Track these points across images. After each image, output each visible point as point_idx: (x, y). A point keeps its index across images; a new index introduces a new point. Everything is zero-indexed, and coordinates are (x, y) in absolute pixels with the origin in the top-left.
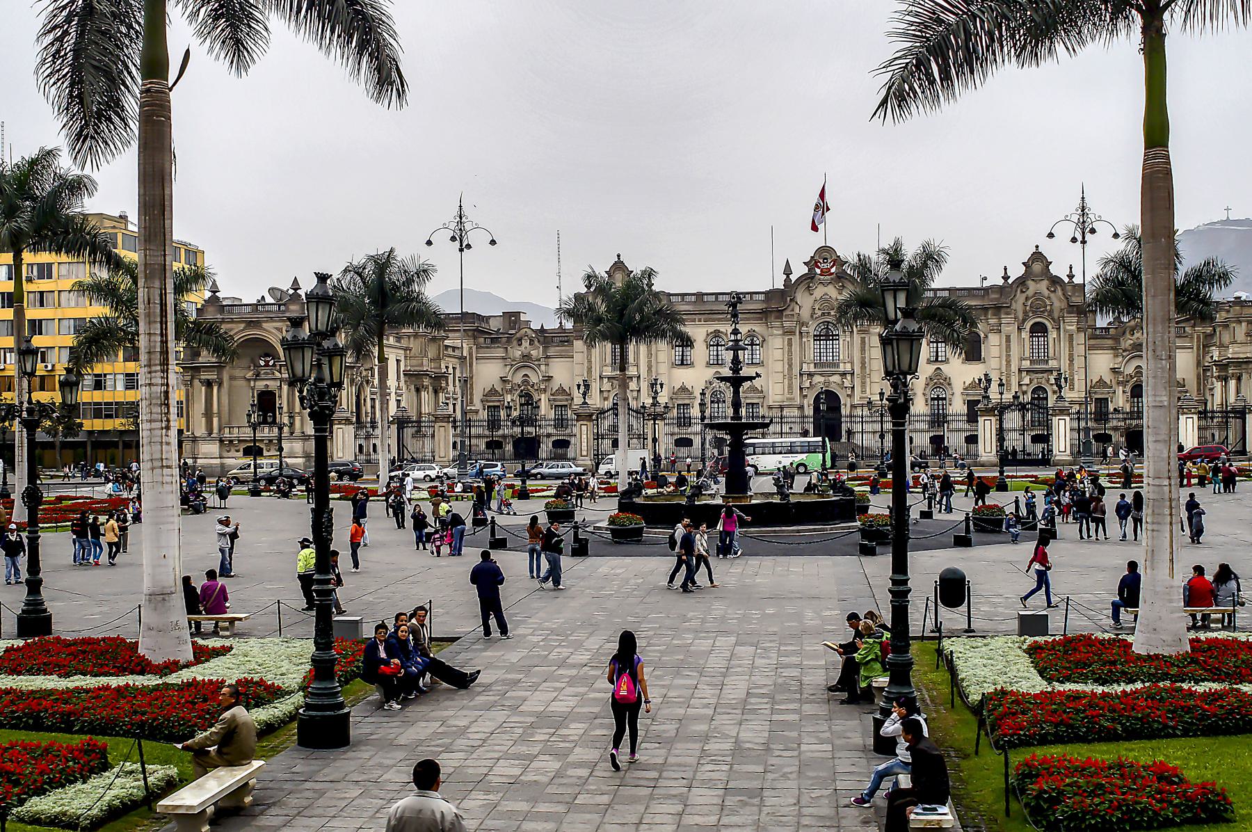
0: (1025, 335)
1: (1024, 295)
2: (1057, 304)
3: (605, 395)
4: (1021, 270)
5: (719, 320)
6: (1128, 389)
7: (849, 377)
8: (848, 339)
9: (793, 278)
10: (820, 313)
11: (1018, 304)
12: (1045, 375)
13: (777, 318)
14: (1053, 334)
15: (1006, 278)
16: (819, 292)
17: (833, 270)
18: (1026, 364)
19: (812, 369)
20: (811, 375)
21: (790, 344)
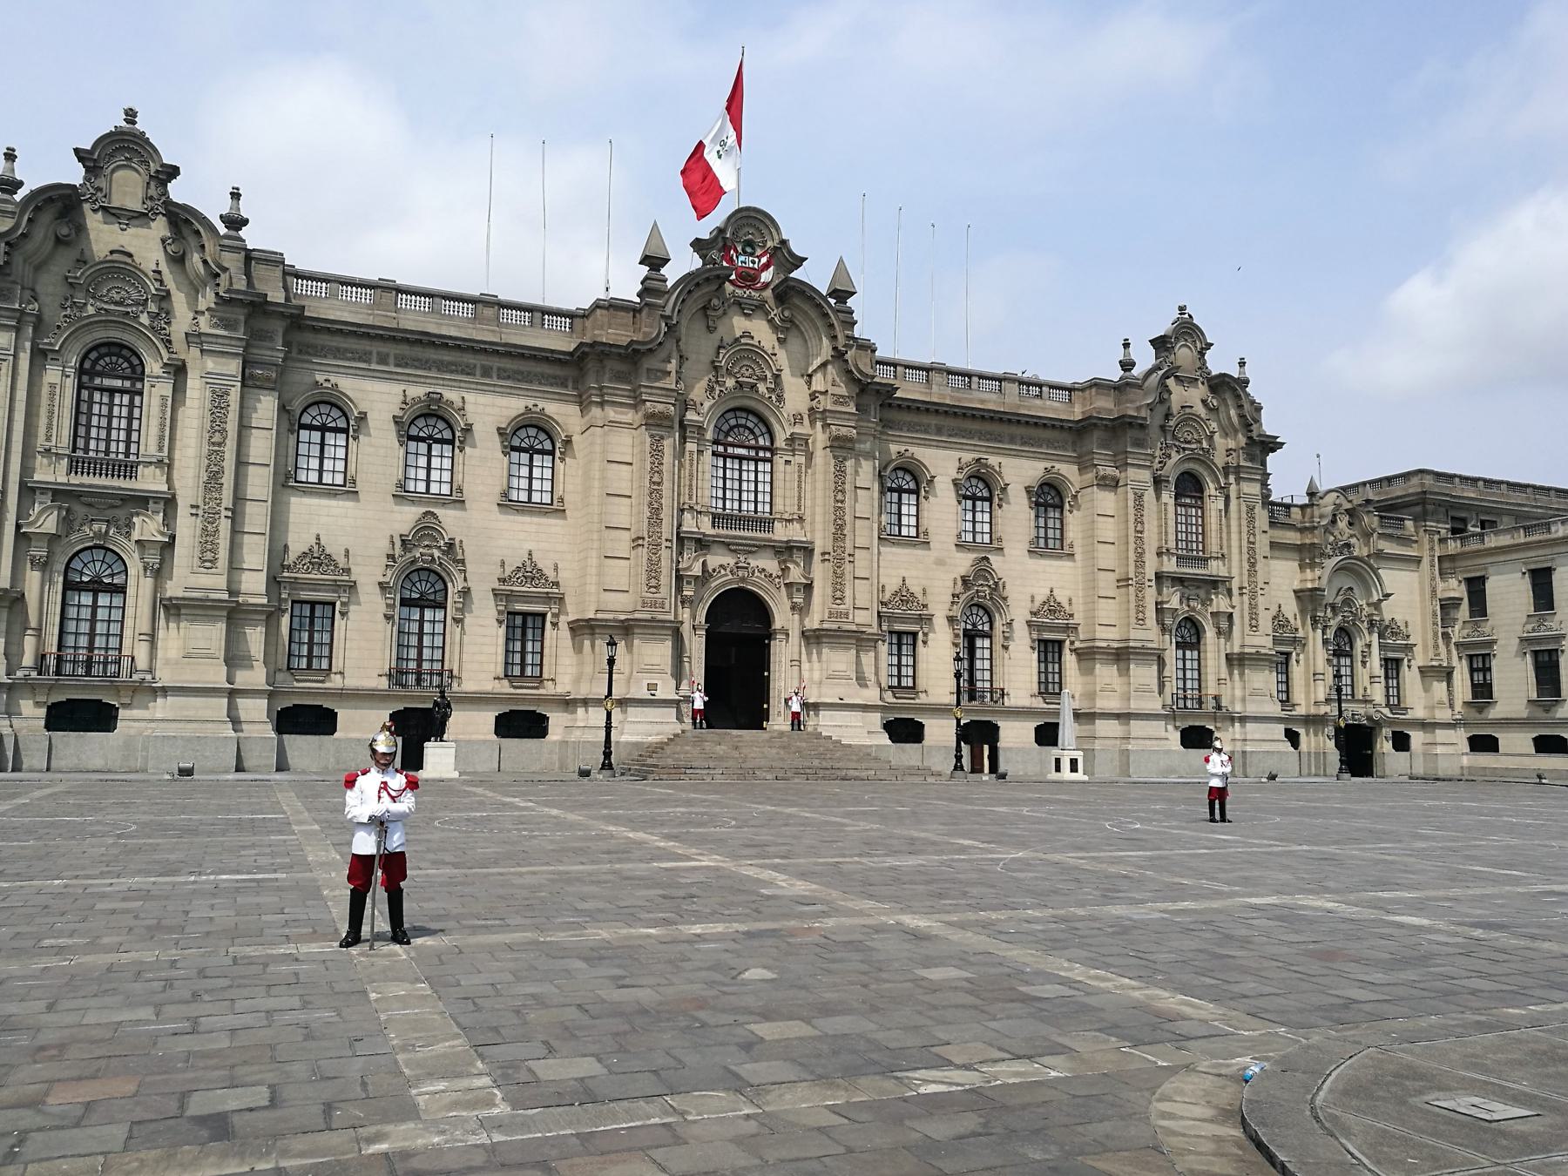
0: (1168, 497)
5: (442, 367)
6: (1330, 634)
7: (798, 557)
10: (730, 383)
11: (1154, 432)
12: (1202, 593)
13: (619, 377)
14: (1214, 505)
15: (1127, 365)
17: (766, 276)
18: (1170, 565)
19: (706, 526)
20: (703, 544)
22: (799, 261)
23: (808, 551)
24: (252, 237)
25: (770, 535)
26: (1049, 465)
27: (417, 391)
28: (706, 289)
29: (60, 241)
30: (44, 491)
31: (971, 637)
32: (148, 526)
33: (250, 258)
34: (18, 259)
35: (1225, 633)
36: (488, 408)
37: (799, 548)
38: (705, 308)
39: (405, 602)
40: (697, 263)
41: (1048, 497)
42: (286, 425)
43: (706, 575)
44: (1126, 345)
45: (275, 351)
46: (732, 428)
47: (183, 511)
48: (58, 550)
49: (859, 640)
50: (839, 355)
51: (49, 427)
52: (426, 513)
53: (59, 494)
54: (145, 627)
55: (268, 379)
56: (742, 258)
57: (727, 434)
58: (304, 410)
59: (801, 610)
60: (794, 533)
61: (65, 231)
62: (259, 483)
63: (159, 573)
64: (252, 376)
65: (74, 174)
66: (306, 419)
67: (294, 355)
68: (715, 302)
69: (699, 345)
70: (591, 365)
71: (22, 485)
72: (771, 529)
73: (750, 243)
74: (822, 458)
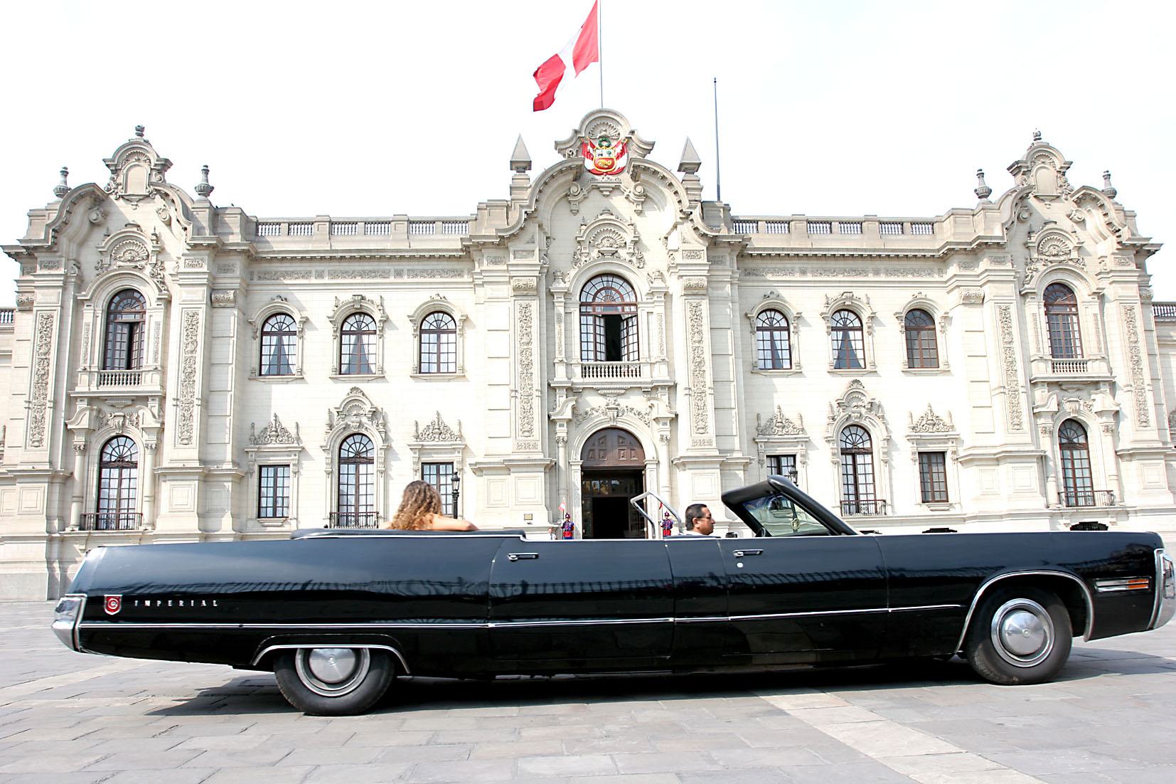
0: (1035, 308)
1: (1024, 229)
2: (1088, 246)
3: (79, 440)
4: (1010, 182)
8: (660, 309)
9: (534, 174)
10: (595, 254)
11: (1017, 250)
15: (984, 194)
16: (591, 207)
17: (621, 163)
20: (571, 390)
21: (526, 318)
22: (649, 147)
23: (673, 388)
24: (217, 199)
25: (638, 379)
26: (916, 292)
27: (346, 297)
28: (562, 180)
29: (93, 225)
30: (82, 399)
31: (851, 453)
32: (147, 416)
33: (216, 214)
34: (63, 240)
35: (1113, 431)
36: (400, 301)
37: (663, 387)
38: (567, 195)
39: (342, 461)
40: (560, 158)
41: (918, 321)
42: (251, 334)
43: (578, 417)
44: (981, 174)
45: (232, 281)
46: (599, 291)
47: (169, 402)
48: (94, 440)
49: (722, 464)
50: (687, 216)
51: (86, 354)
52: (352, 389)
53: (92, 400)
54: (147, 492)
55: (228, 300)
56: (598, 152)
57: (595, 296)
58: (266, 321)
59: (669, 441)
60: (660, 374)
61: (94, 216)
62: (228, 378)
63: (157, 450)
64: (218, 300)
65: (102, 178)
66: (267, 328)
67: (255, 281)
68: (574, 189)
69: (566, 227)
70: (475, 255)
71: (68, 396)
72: (638, 373)
73: (605, 138)
74: (679, 303)
